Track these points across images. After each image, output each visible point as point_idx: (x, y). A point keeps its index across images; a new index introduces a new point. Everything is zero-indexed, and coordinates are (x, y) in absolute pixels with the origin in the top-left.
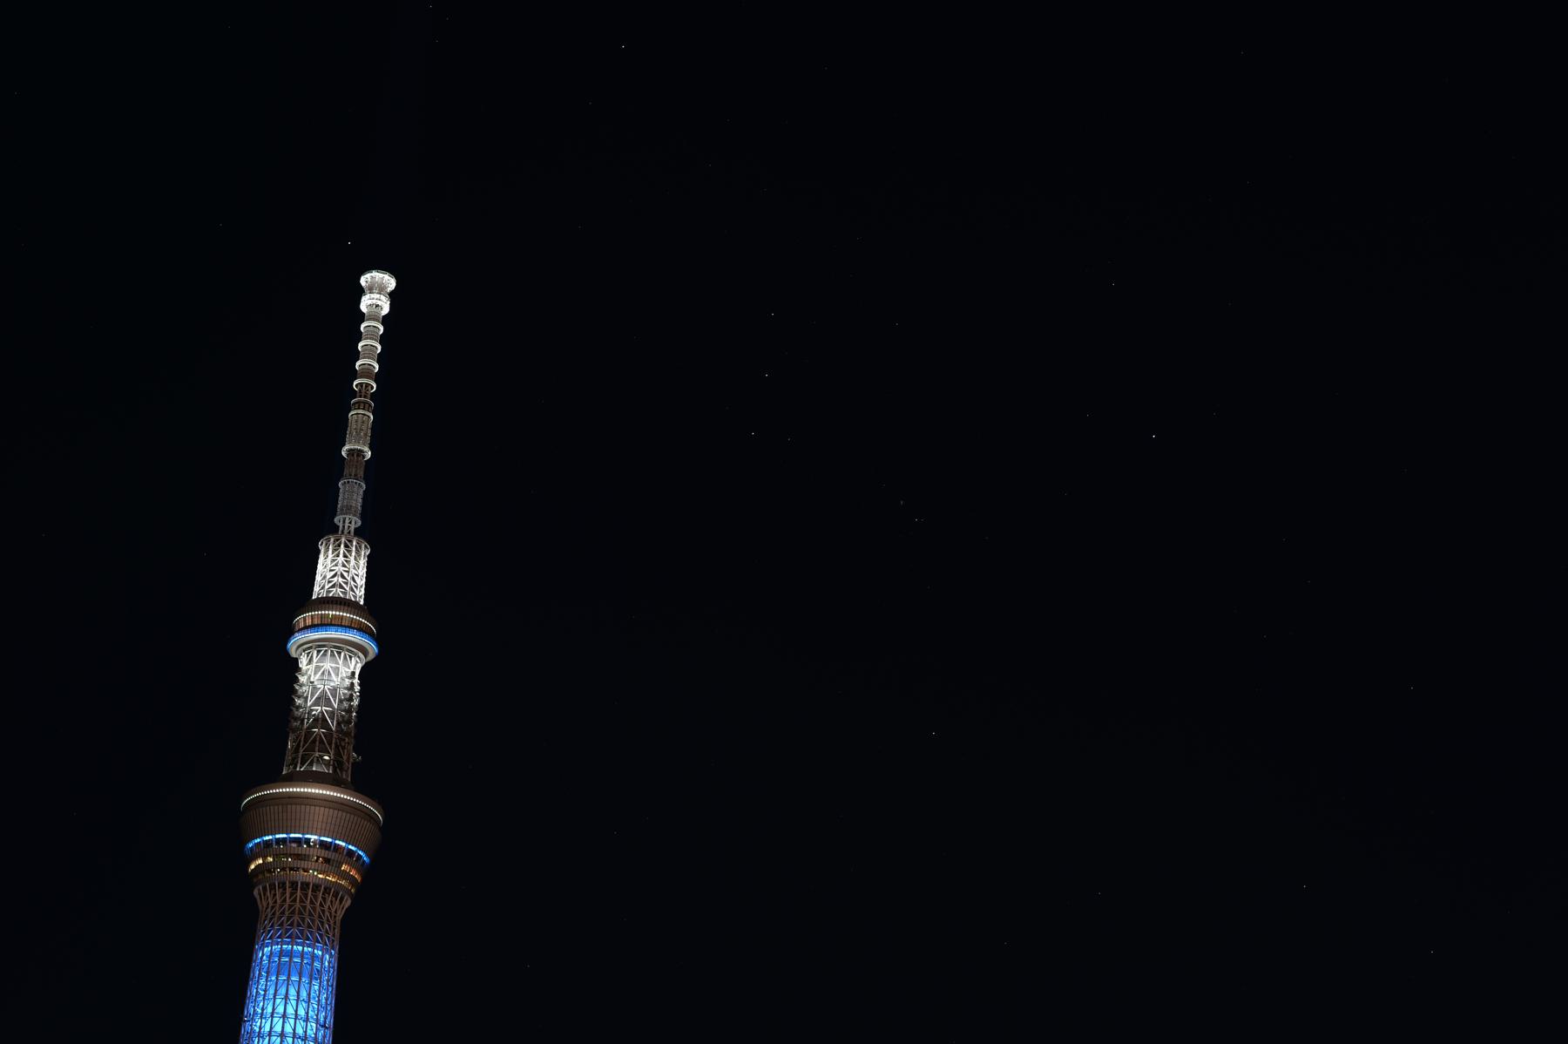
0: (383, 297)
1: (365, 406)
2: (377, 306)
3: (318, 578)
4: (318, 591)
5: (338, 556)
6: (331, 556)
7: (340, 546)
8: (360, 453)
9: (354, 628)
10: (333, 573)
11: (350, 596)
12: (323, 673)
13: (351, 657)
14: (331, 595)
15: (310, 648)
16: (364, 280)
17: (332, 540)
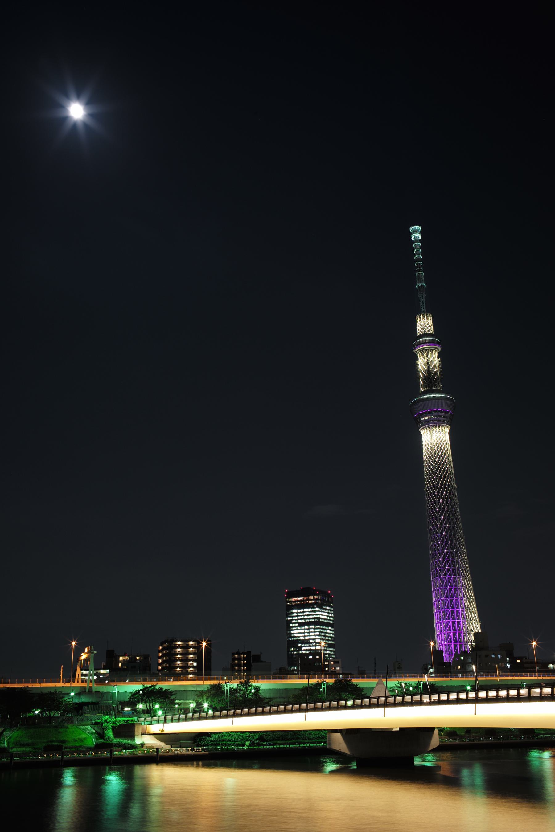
0: (419, 234)
1: (421, 270)
2: (417, 237)
3: (418, 328)
4: (419, 332)
5: (425, 320)
6: (422, 320)
7: (424, 316)
8: (422, 286)
9: (435, 343)
11: (430, 332)
12: (433, 358)
13: (435, 352)
14: (425, 333)
15: (423, 350)
16: (411, 230)
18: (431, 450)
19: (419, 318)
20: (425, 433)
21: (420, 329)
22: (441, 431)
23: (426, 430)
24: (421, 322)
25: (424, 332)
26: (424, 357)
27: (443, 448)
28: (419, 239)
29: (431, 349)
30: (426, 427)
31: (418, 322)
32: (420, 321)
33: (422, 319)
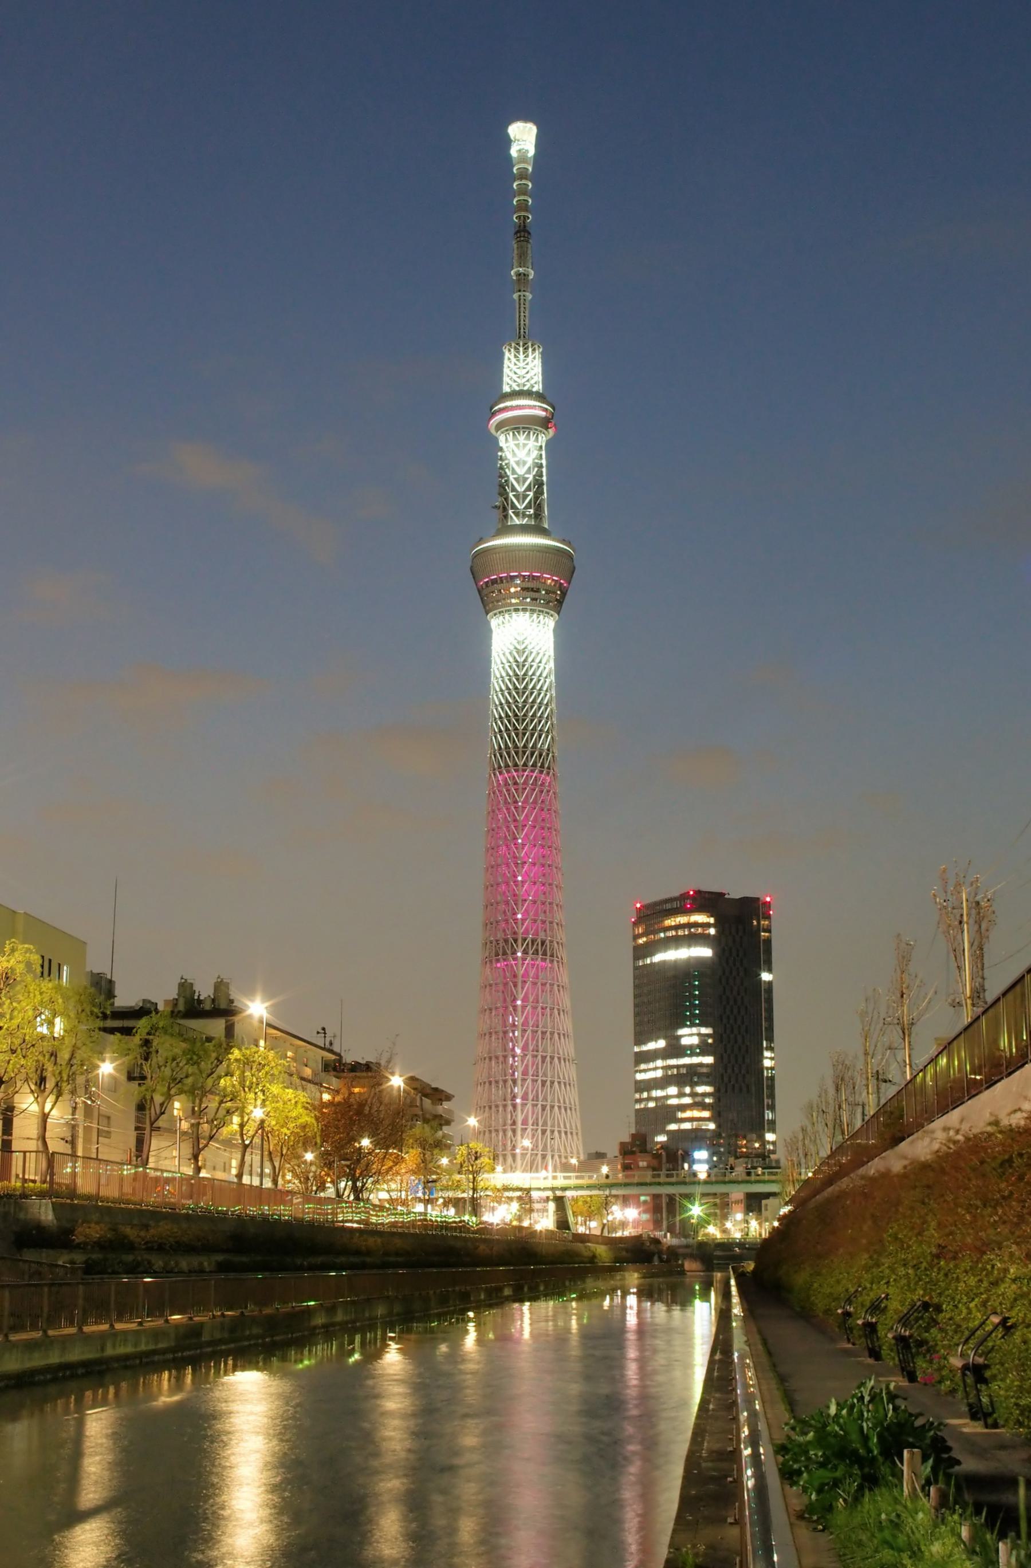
5: (527, 356)
6: (521, 356)
7: (528, 347)
10: (525, 371)
14: (525, 388)
17: (521, 344)
18: (518, 666)
19: (512, 350)
20: (503, 623)
21: (515, 377)
22: (541, 625)
23: (507, 616)
24: (518, 360)
25: (524, 385)
26: (517, 445)
27: (542, 665)
28: (532, 152)
29: (536, 430)
30: (509, 611)
31: (509, 359)
32: (515, 356)
33: (521, 353)
